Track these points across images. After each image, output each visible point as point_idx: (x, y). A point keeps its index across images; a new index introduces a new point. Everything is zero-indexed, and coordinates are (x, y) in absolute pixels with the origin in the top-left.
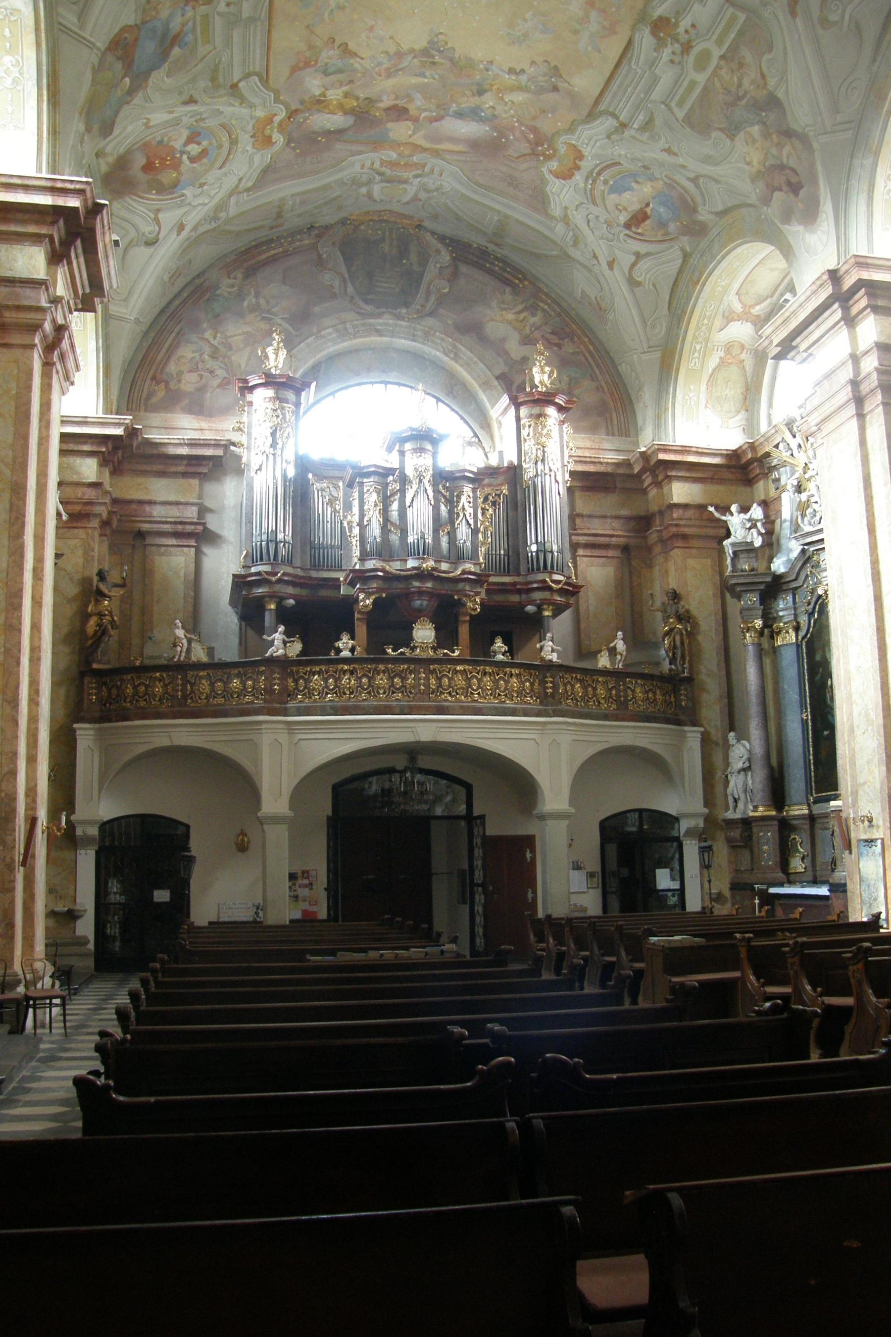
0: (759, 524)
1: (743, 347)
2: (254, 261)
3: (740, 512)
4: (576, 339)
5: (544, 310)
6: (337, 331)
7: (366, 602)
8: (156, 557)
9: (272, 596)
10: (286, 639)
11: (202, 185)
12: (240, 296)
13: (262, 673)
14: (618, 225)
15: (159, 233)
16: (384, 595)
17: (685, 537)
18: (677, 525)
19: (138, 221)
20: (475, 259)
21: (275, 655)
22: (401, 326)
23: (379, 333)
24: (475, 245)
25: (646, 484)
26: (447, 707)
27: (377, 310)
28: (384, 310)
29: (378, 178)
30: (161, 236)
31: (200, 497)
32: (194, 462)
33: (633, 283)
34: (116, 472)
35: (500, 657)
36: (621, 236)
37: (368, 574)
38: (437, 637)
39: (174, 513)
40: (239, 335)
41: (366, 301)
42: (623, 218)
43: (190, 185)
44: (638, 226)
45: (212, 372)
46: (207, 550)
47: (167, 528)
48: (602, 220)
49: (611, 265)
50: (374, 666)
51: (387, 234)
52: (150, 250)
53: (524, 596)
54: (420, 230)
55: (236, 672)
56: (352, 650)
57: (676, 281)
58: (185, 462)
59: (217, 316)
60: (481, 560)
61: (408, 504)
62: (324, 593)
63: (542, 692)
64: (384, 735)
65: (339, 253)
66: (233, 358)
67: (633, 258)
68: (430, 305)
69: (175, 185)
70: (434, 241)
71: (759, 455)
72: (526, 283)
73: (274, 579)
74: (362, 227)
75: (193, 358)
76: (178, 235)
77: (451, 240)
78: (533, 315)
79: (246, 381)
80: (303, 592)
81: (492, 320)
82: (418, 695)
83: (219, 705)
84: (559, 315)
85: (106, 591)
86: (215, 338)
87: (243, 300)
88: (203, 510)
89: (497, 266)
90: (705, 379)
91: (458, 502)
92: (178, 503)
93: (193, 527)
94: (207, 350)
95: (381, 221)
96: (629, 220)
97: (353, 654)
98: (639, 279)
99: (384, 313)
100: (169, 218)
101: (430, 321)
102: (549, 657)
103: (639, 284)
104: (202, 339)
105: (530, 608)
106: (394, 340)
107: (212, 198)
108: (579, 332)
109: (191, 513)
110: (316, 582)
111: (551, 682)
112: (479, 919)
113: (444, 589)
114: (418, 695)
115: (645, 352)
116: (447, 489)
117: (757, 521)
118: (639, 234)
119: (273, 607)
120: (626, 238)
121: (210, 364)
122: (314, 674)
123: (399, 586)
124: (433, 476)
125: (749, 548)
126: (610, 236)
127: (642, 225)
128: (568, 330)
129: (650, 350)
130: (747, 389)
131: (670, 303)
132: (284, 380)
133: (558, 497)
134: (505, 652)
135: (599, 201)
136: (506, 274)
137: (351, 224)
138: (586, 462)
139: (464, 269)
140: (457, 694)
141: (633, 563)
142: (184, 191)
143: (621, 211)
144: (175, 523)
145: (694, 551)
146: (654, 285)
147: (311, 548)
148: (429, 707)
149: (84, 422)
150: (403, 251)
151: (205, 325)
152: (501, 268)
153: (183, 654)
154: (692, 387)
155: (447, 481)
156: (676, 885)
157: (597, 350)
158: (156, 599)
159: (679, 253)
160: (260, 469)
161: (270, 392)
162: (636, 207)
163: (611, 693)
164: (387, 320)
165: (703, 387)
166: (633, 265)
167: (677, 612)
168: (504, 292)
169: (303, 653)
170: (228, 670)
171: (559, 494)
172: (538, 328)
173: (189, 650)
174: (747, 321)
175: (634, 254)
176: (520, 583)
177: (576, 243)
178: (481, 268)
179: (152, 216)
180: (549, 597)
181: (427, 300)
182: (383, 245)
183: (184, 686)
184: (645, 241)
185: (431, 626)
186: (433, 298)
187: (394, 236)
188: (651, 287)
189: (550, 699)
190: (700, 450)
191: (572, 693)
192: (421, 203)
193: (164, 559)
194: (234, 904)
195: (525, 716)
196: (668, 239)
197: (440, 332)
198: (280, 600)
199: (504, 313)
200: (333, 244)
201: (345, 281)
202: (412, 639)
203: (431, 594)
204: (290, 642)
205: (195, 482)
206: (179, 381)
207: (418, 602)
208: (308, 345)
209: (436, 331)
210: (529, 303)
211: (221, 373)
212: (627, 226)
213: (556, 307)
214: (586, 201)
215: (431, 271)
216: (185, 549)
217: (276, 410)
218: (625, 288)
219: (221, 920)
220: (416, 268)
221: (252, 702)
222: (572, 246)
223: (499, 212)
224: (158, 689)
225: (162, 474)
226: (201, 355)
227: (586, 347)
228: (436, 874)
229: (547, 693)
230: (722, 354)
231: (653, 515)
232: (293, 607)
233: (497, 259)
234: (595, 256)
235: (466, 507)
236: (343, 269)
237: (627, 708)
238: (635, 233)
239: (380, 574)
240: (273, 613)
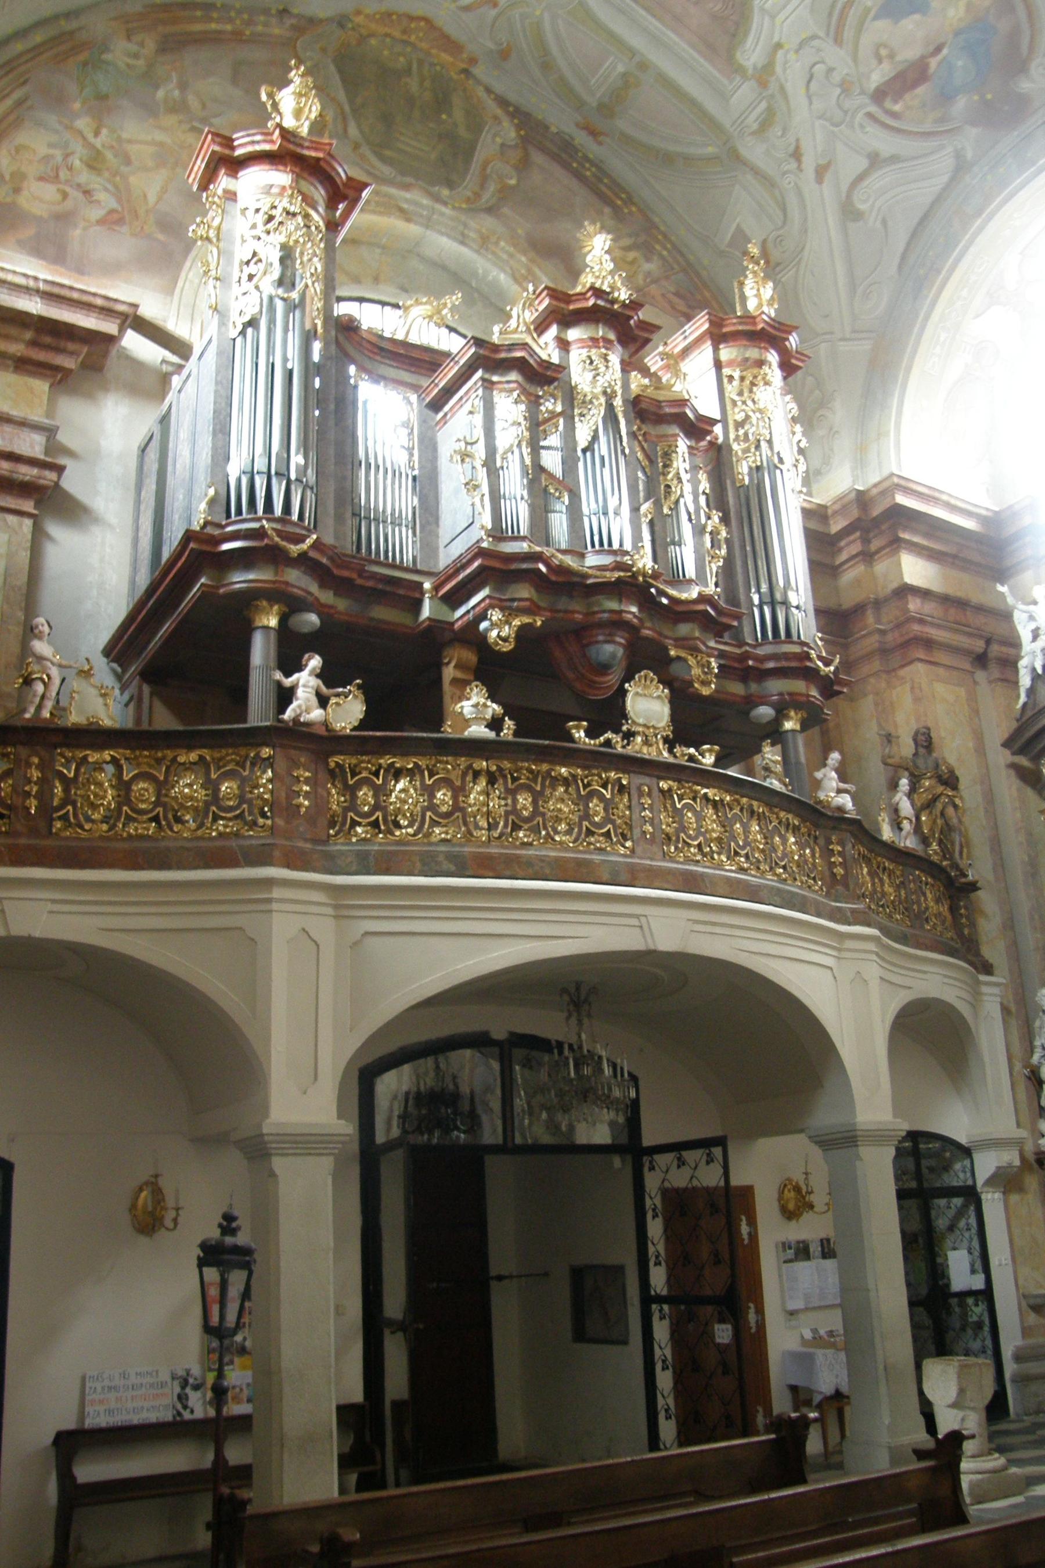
9: (276, 595)
10: (324, 690)
12: (150, 78)
13: (269, 762)
14: (863, 92)
16: (539, 623)
17: (929, 644)
18: (921, 621)
22: (442, 214)
23: (406, 216)
24: (554, 129)
25: (844, 556)
27: (399, 178)
28: (408, 180)
31: (50, 413)
32: (48, 340)
33: (849, 212)
37: (514, 566)
38: (674, 718)
40: (146, 143)
41: (383, 159)
42: (876, 78)
44: (898, 97)
45: (87, 193)
46: (55, 530)
48: (836, 78)
49: (820, 173)
50: (545, 767)
54: (467, 78)
55: (193, 756)
56: (495, 724)
58: (28, 335)
59: (102, 98)
62: (383, 613)
63: (827, 873)
64: (581, 930)
65: (332, 68)
66: (132, 180)
67: (863, 163)
68: (488, 195)
70: (490, 102)
72: (634, 209)
73: (294, 549)
74: (373, 41)
75: (47, 158)
77: (517, 110)
78: (648, 260)
79: (228, 142)
80: (342, 605)
83: (141, 837)
86: (97, 134)
87: (157, 87)
88: (53, 446)
93: (35, 471)
94: (79, 150)
95: (405, 42)
96: (888, 83)
97: (498, 735)
98: (862, 207)
101: (488, 222)
104: (69, 128)
106: (428, 232)
109: (32, 445)
110: (370, 584)
112: (665, 1380)
118: (894, 115)
119: (273, 622)
121: (84, 177)
122: (398, 774)
123: (576, 609)
127: (907, 97)
128: (699, 297)
129: (856, 335)
131: (904, 257)
132: (321, 155)
135: (848, 34)
137: (353, 29)
143: (880, 61)
145: (941, 671)
146: (884, 222)
147: (354, 515)
148: (670, 872)
150: (442, 102)
151: (77, 105)
152: (594, 175)
153: (49, 704)
156: (978, 1282)
161: (281, 178)
162: (910, 54)
164: (414, 197)
166: (861, 178)
169: (363, 725)
170: (170, 754)
172: (655, 281)
177: (766, 123)
178: (566, 166)
180: (804, 691)
181: (482, 186)
182: (408, 80)
183: (45, 783)
186: (492, 187)
188: (878, 225)
190: (953, 501)
192: (494, 12)
194: (124, 1375)
200: (324, 50)
202: (625, 716)
204: (338, 695)
205: (41, 386)
206: (17, 190)
207: (609, 648)
211: (107, 200)
212: (879, 95)
213: (680, 259)
214: (822, 34)
215: (487, 147)
216: (11, 519)
217: (294, 215)
219: (89, 1423)
220: (462, 132)
221: (237, 835)
222: (753, 133)
223: (632, 52)
226: (67, 156)
228: (500, 1278)
229: (834, 875)
231: (859, 609)
233: (586, 158)
234: (797, 155)
239: (543, 568)
240: (273, 636)
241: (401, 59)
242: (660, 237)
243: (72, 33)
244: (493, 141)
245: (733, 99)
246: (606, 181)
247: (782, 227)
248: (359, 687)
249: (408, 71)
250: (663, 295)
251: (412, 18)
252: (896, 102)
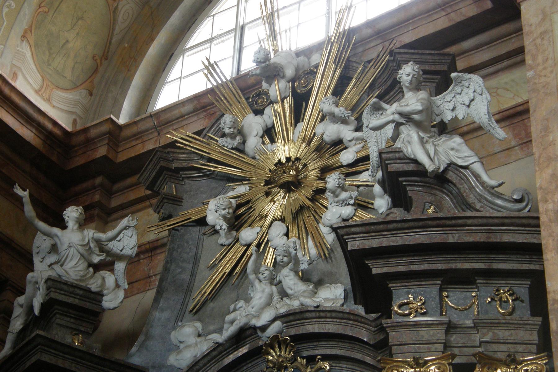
0: (120, 266)
3: (82, 224)
71: (122, 157)
117: (120, 257)
125: (88, 305)
130: (105, 56)
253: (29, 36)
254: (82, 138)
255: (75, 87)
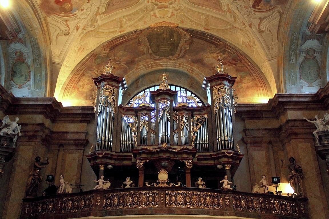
1: (314, 51)
2: (114, 44)
4: (242, 61)
5: (229, 52)
6: (145, 66)
7: (140, 164)
8: (68, 154)
10: (104, 181)
11: (82, 10)
14: (250, 7)
15: (69, 31)
17: (296, 134)
19: (59, 25)
20: (200, 36)
21: (97, 188)
22: (170, 62)
26: (174, 211)
27: (160, 58)
28: (163, 57)
29: (156, 7)
30: (70, 32)
33: (261, 32)
34: (54, 121)
35: (201, 187)
36: (252, 12)
39: (76, 136)
41: (157, 55)
43: (78, 10)
47: (72, 142)
49: (250, 26)
51: (165, 31)
52: (67, 37)
53: (216, 161)
57: (279, 26)
58: (81, 116)
60: (192, 144)
61: (159, 121)
62: (126, 162)
67: (259, 21)
68: (182, 54)
69: (71, 10)
72: (221, 43)
73: (101, 156)
74: (155, 29)
76: (77, 31)
77: (190, 30)
78: (224, 54)
81: (207, 57)
82: (160, 205)
84: (234, 53)
85: (38, 166)
89: (209, 38)
90: (298, 67)
91: (182, 120)
92: (77, 133)
95: (163, 27)
97: (131, 186)
99: (163, 58)
100: (72, 24)
102: (226, 187)
103: (263, 32)
105: (219, 166)
107: (88, 15)
108: (244, 58)
109: (83, 136)
111: (228, 199)
113: (175, 157)
114: (160, 205)
115: (270, 60)
116: (177, 115)
118: (259, 9)
120: (255, 12)
124: (170, 110)
126: (248, 13)
127: (260, 5)
129: (272, 59)
131: (278, 38)
132: (111, 77)
133: (230, 118)
134: (204, 184)
136: (212, 41)
137: (151, 29)
138: (247, 107)
139: (195, 40)
140: (179, 204)
141: (274, 149)
142: (76, 13)
144: (75, 140)
145: (301, 140)
149: (37, 100)
152: (210, 38)
153: (63, 190)
154: (292, 71)
155: (177, 111)
157: (252, 65)
158: (65, 171)
159: (278, 14)
160: (101, 112)
163: (261, 205)
165: (298, 70)
167: (295, 167)
168: (212, 47)
171: (231, 116)
173: (65, 189)
174: (314, 39)
175: (259, 19)
176: (213, 155)
179: (65, 23)
181: (180, 53)
182: (164, 35)
183: (61, 204)
184: (261, 12)
185: (166, 172)
186: (183, 51)
187: (168, 31)
188: (269, 32)
189: (228, 207)
191: (240, 205)
192: (175, 16)
193: (70, 155)
195: (214, 215)
196: (272, 9)
197: (186, 63)
198: (106, 165)
199: (212, 54)
201: (148, 49)
202: (157, 179)
203: (168, 159)
208: (133, 72)
209: (184, 63)
210: (222, 50)
212: (254, 6)
215: (182, 43)
216: (79, 151)
218: (258, 35)
223: (204, 14)
224: (51, 206)
225: (72, 122)
227: (247, 64)
230: (305, 55)
232: (112, 169)
233: (208, 35)
234: (244, 24)
235: (185, 121)
236: (148, 45)
237: (270, 213)
238: (258, 9)
241: (162, 30)
242: (228, 47)
243: (94, 54)
244: (184, 40)
245: (227, 17)
246: (213, 39)
247: (249, 39)
248: (109, 181)
249: (163, 33)
250: (228, 61)
251: (162, 22)
252: (258, 7)
253: (301, 78)
254: (318, 94)
255: (316, 79)
